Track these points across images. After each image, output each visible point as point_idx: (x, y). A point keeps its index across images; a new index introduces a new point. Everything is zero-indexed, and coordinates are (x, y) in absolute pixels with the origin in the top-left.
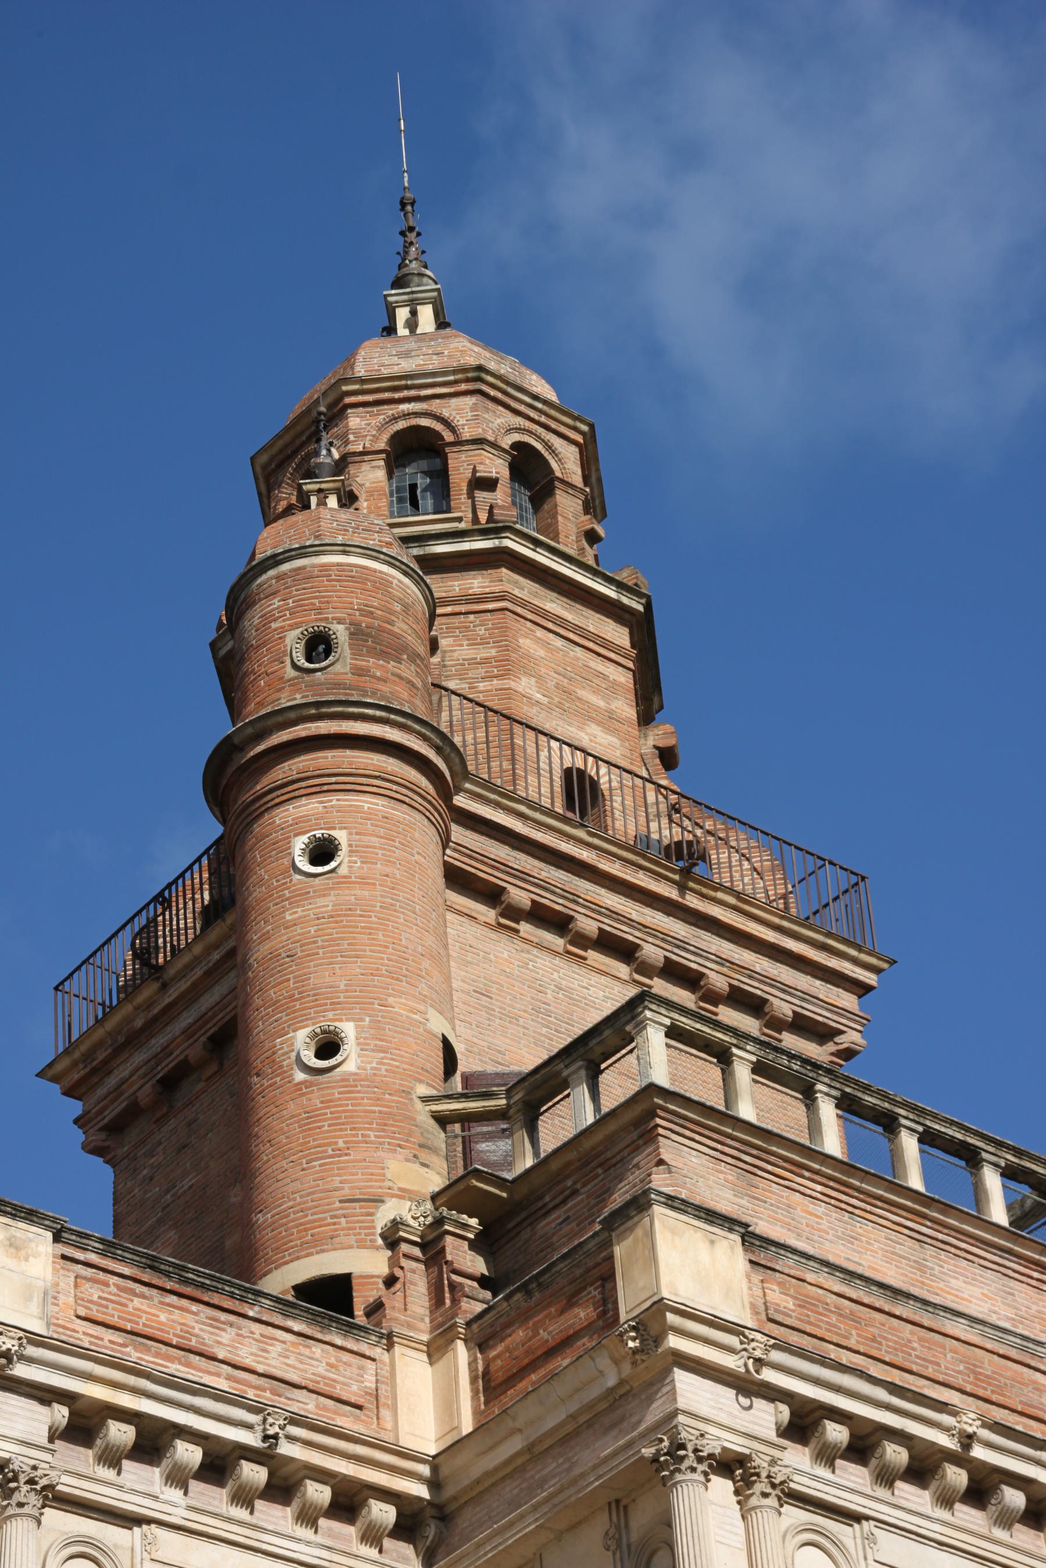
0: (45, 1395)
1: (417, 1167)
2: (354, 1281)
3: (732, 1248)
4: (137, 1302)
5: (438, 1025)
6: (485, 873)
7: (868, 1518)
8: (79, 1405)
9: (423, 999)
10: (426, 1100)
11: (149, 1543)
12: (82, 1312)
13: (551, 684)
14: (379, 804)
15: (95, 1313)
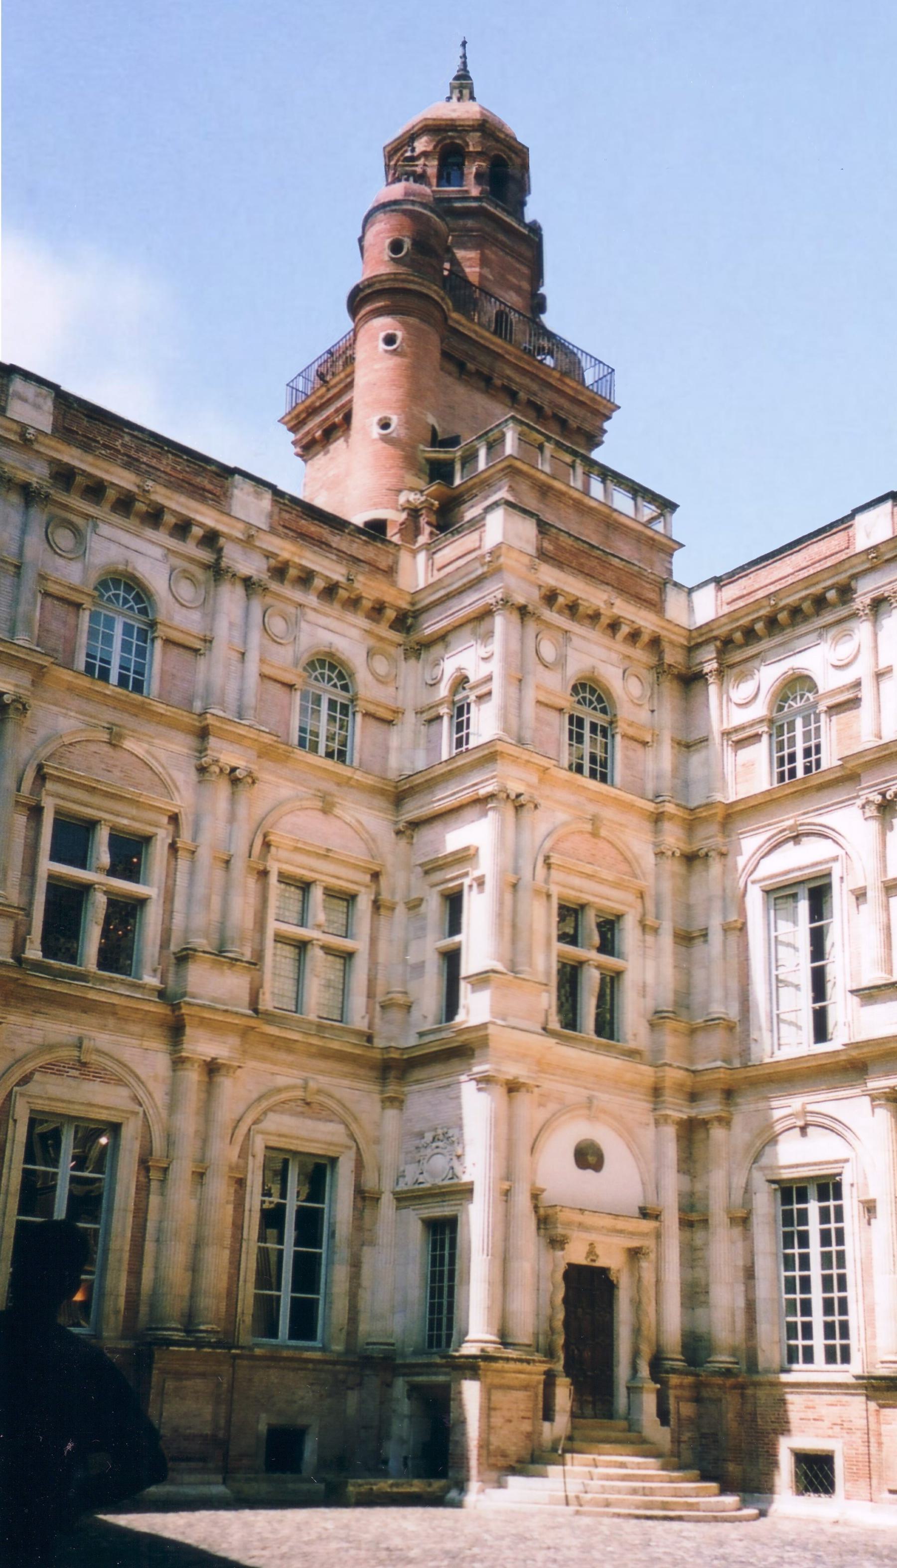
0: (268, 555)
2: (388, 523)
5: (431, 420)
6: (457, 355)
8: (280, 559)
11: (304, 614)
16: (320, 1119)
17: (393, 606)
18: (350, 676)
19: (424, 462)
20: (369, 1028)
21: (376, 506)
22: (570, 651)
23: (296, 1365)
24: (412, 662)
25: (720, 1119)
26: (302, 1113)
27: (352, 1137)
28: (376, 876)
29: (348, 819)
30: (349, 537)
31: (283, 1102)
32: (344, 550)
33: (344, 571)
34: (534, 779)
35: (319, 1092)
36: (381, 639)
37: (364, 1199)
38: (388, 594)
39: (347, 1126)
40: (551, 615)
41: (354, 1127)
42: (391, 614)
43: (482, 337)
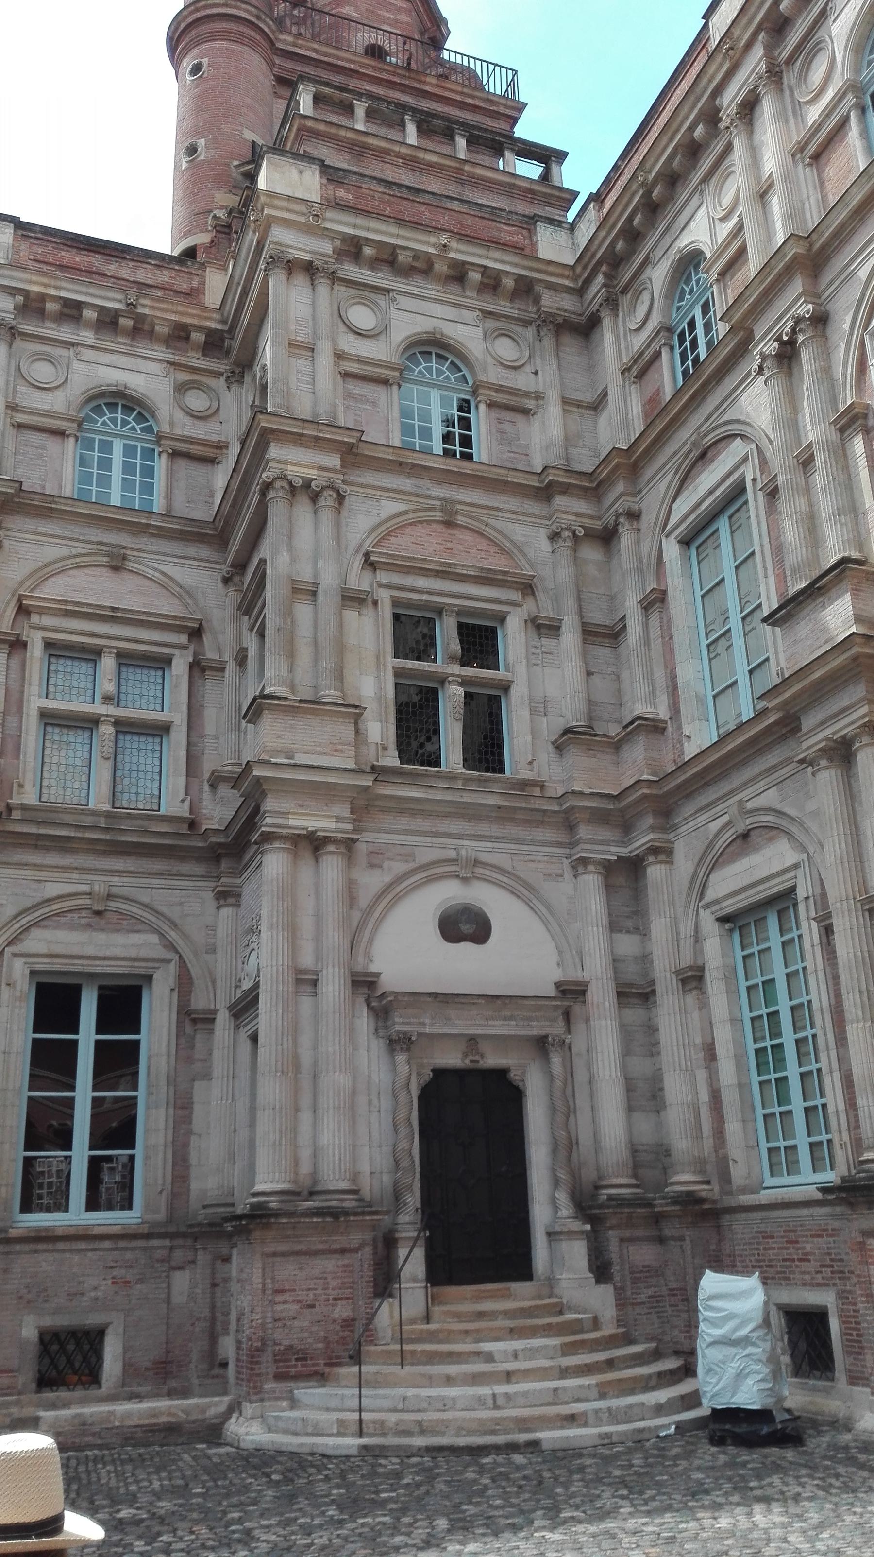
1: (231, 195)
3: (313, 173)
4: (63, 253)
7: (393, 290)
9: (242, 125)
10: (237, 167)
12: (32, 257)
13: (363, 9)
14: (225, 44)
15: (39, 257)
16: (118, 931)
17: (199, 328)
18: (153, 416)
19: (240, 178)
20: (191, 813)
21: (186, 234)
22: (394, 313)
23: (82, 1245)
24: (235, 387)
25: (655, 851)
26: (89, 926)
27: (171, 946)
28: (196, 633)
29: (150, 572)
30: (131, 264)
31: (57, 915)
32: (125, 276)
33: (119, 296)
34: (334, 461)
35: (110, 896)
36: (194, 370)
37: (194, 1021)
38: (189, 316)
39: (162, 935)
40: (350, 271)
41: (173, 935)
42: (198, 337)
43: (326, 55)
